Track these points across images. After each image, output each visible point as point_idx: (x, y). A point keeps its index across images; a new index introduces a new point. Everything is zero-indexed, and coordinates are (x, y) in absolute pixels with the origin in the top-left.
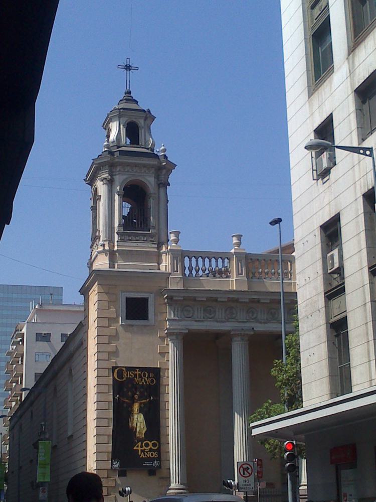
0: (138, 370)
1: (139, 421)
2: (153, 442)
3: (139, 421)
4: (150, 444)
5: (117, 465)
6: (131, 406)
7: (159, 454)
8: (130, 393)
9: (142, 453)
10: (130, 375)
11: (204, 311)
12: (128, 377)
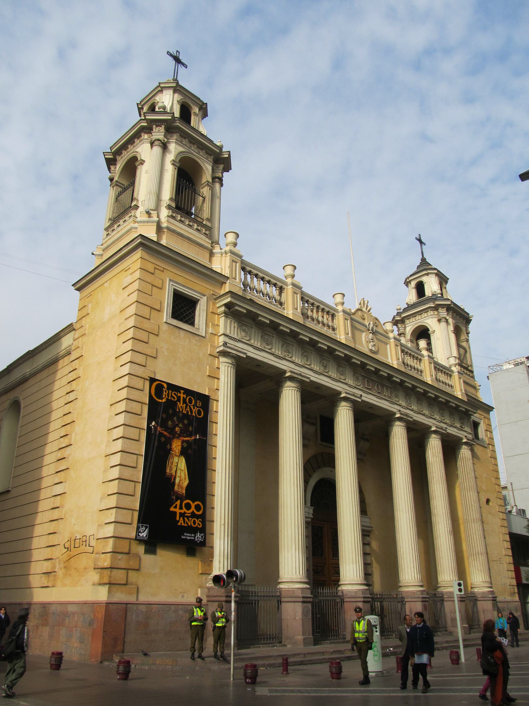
0: (182, 391)
1: (179, 468)
2: (196, 503)
3: (179, 468)
4: (193, 505)
5: (144, 534)
6: (169, 441)
7: (204, 522)
8: (170, 423)
9: (182, 518)
10: (172, 396)
11: (261, 338)
12: (170, 398)
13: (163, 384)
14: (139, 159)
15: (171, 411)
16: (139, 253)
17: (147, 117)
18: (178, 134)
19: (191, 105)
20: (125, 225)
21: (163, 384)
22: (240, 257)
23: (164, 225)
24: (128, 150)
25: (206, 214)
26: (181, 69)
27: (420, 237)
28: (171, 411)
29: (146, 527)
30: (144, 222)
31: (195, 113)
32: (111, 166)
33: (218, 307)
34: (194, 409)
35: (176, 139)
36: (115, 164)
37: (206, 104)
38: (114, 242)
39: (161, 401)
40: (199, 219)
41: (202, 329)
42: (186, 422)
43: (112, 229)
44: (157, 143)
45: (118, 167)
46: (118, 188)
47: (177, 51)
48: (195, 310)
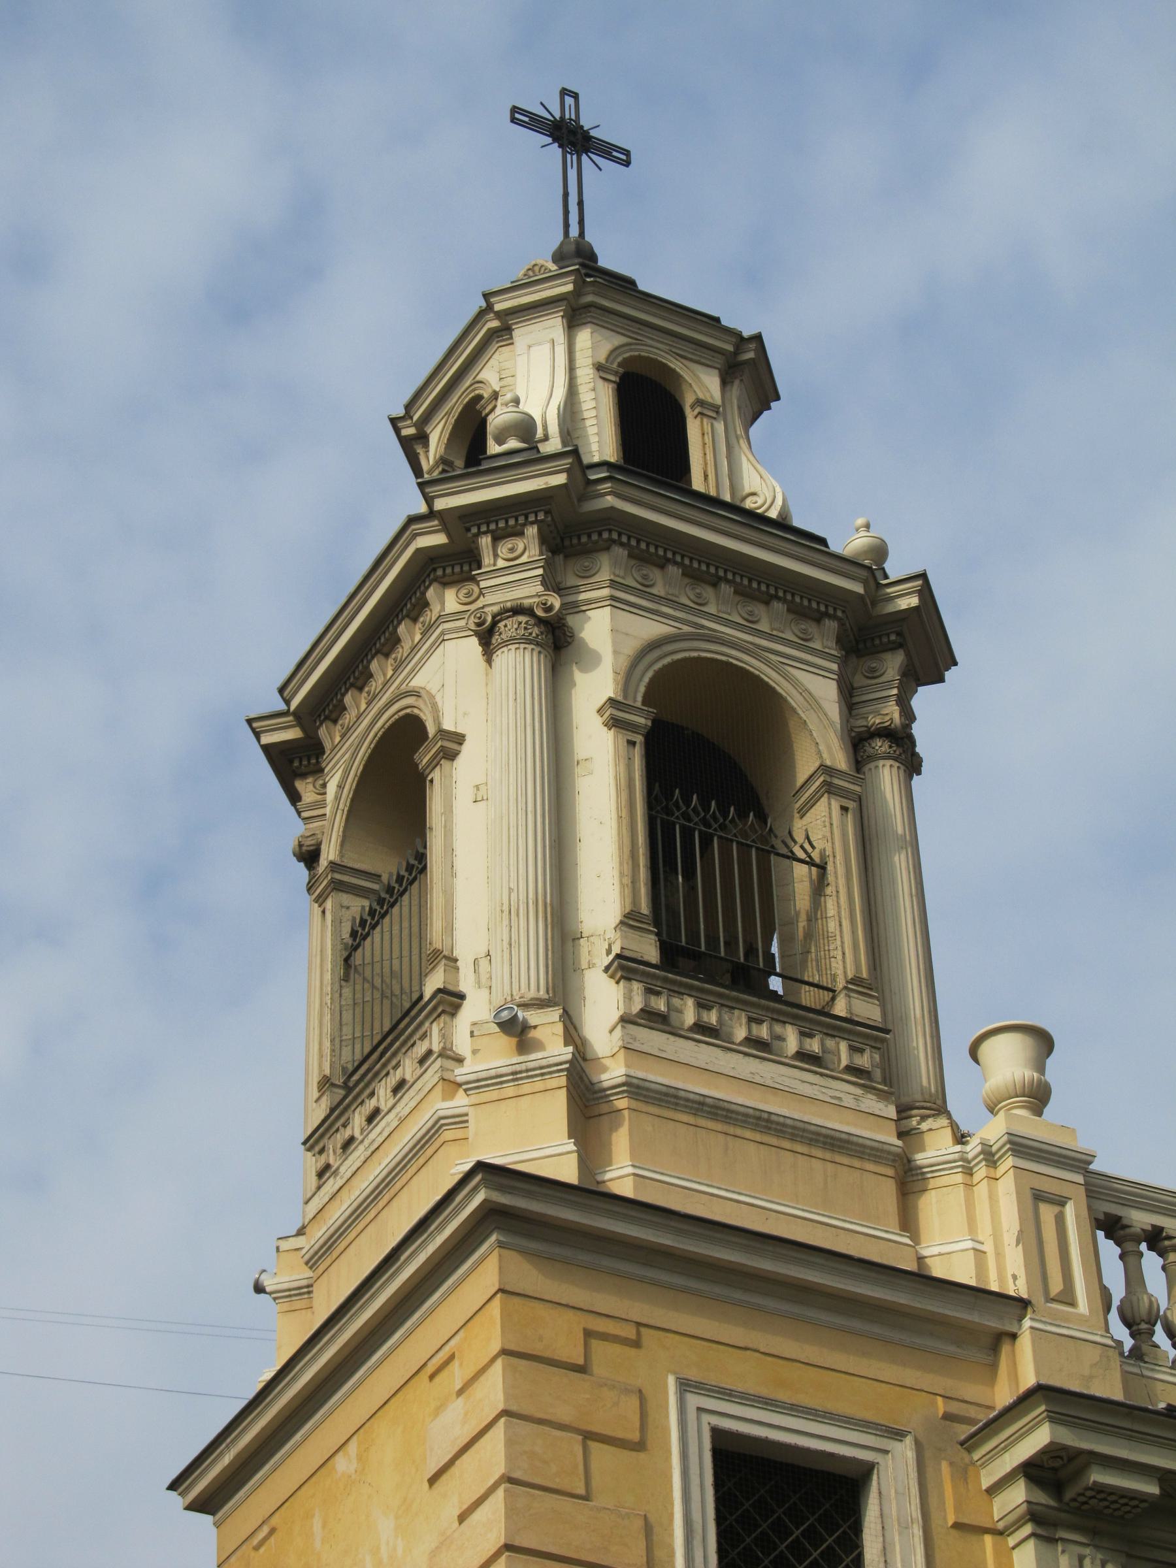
14: (431, 730)
16: (485, 1271)
17: (440, 504)
18: (620, 552)
19: (675, 364)
20: (403, 1108)
22: (1079, 1162)
23: (613, 1072)
24: (374, 685)
25: (841, 953)
26: (598, 175)
30: (496, 1080)
31: (700, 402)
32: (300, 785)
33: (994, 1490)
35: (613, 584)
36: (319, 771)
37: (758, 338)
38: (358, 1212)
40: (809, 997)
43: (340, 1138)
44: (509, 627)
45: (332, 788)
46: (346, 899)
47: (564, 92)
48: (857, 1528)
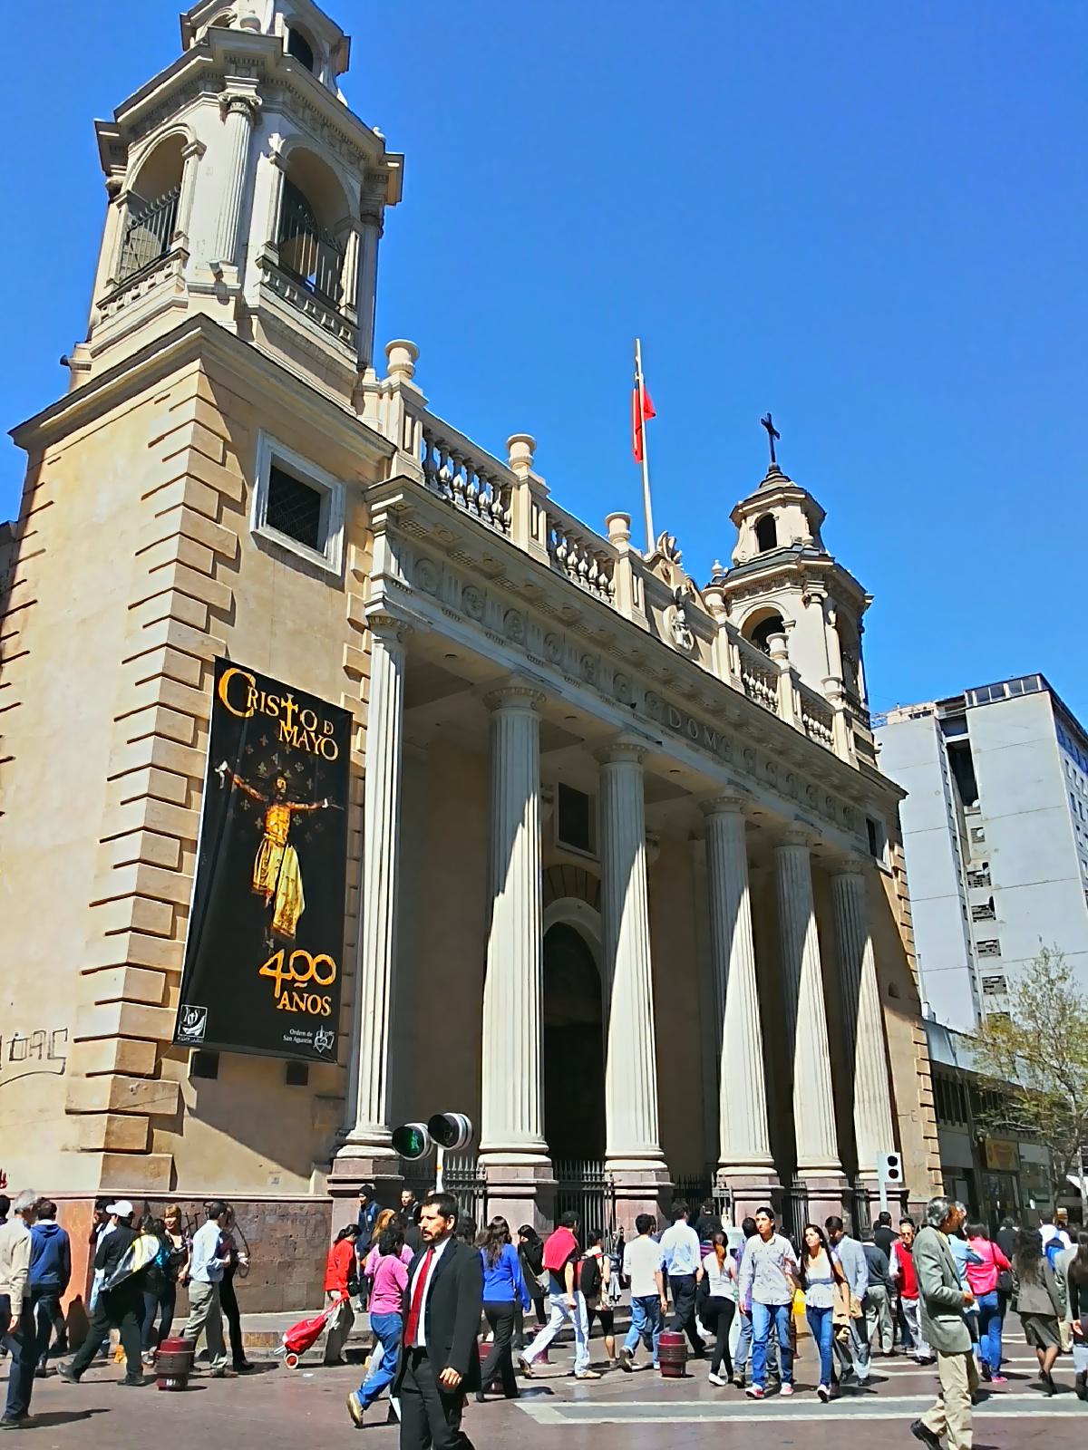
4: (313, 963)
8: (262, 768)
10: (266, 705)
12: (262, 710)
13: (248, 675)
15: (264, 741)
21: (248, 675)
27: (770, 420)
28: (264, 741)
29: (202, 1013)
34: (317, 738)
39: (240, 714)
41: (335, 559)
42: (299, 767)
